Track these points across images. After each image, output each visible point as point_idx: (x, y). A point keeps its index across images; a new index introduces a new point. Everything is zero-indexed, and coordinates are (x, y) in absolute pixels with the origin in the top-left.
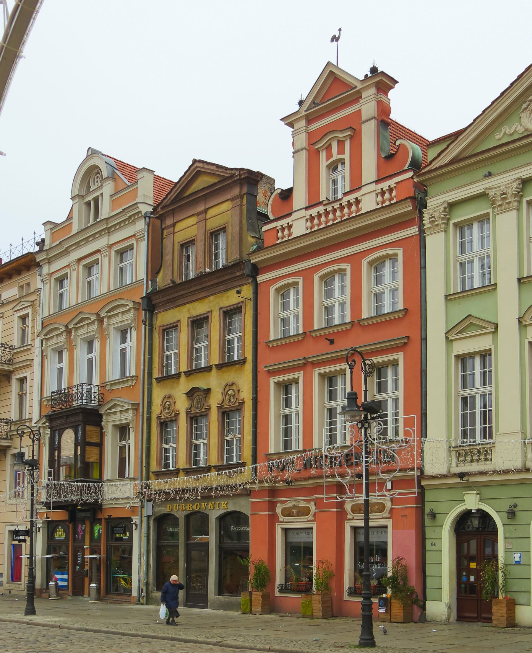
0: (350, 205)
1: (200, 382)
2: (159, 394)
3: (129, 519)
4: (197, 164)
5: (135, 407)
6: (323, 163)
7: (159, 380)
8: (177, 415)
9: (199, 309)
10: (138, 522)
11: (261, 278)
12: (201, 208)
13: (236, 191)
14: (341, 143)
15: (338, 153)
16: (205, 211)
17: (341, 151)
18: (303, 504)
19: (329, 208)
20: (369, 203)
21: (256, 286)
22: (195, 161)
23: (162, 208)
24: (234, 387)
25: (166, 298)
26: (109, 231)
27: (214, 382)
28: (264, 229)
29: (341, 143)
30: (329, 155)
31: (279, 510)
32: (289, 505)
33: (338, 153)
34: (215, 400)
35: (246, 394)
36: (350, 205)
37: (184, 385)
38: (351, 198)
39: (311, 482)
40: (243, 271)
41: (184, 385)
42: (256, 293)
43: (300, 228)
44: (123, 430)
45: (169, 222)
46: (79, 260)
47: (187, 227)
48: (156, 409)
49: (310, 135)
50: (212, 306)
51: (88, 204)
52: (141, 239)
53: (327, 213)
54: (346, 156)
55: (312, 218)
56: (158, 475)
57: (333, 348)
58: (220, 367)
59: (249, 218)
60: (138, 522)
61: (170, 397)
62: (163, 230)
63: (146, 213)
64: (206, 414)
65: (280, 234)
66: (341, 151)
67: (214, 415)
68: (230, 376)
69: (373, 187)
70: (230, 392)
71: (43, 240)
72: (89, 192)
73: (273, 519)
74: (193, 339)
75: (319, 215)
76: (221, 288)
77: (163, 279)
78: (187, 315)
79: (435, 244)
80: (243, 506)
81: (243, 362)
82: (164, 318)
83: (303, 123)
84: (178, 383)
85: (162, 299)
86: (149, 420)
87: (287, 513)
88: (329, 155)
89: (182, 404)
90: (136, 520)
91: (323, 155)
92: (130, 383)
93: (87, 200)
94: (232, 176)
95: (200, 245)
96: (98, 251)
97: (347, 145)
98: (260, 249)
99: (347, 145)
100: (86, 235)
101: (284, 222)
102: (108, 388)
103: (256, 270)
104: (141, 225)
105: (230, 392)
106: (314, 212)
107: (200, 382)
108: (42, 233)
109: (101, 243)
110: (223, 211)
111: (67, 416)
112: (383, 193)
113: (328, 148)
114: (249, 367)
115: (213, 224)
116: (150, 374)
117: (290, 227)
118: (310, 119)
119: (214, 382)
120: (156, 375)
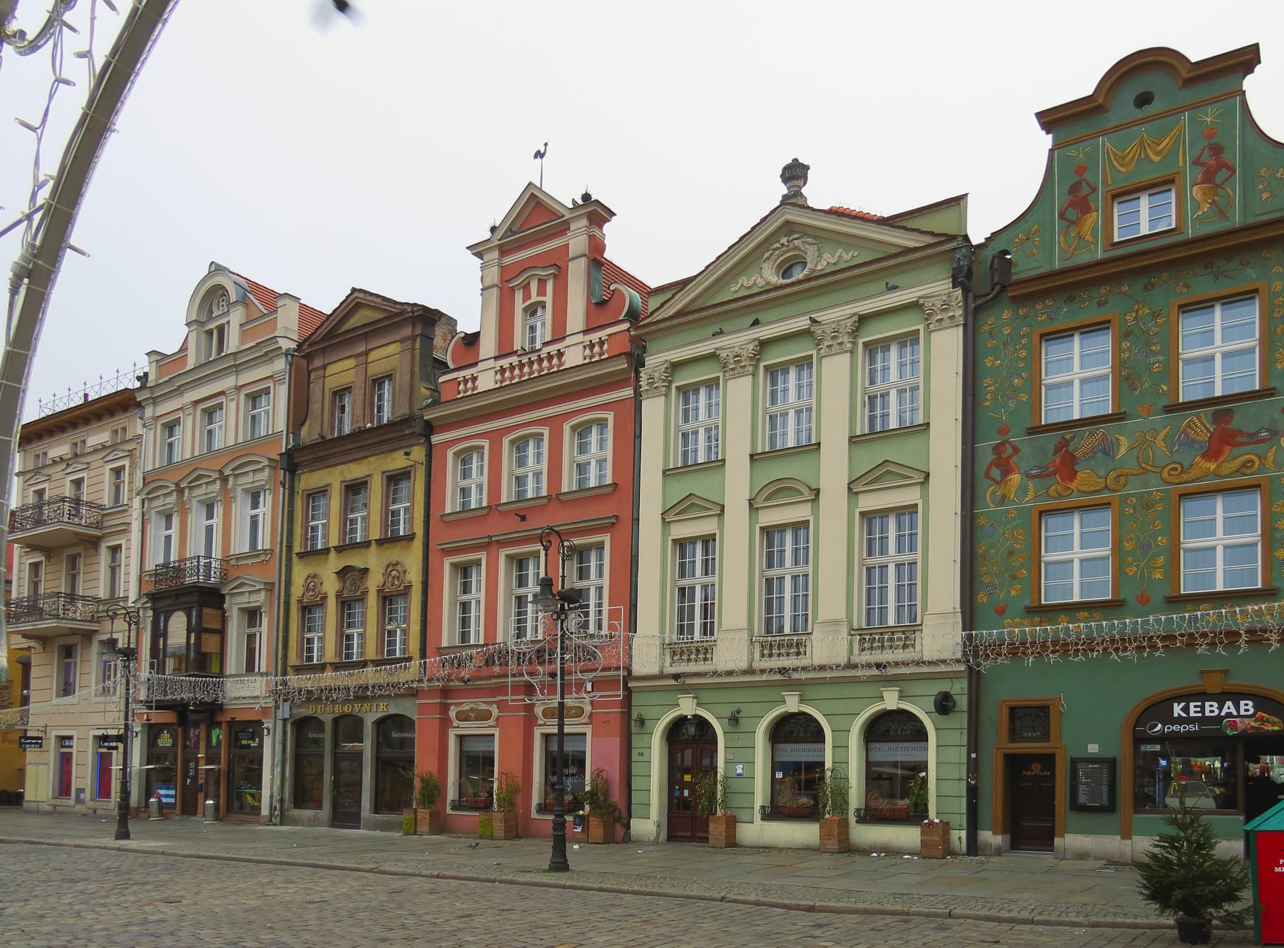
0: (550, 357)
1: (356, 560)
2: (300, 573)
3: (259, 723)
4: (356, 294)
5: (269, 588)
6: (519, 305)
7: (301, 556)
8: (324, 598)
9: (355, 471)
10: (271, 726)
11: (435, 439)
12: (361, 348)
13: (407, 331)
14: (542, 282)
15: (538, 295)
16: (367, 353)
17: (542, 292)
18: (483, 707)
19: (525, 360)
20: (574, 357)
21: (430, 448)
22: (354, 290)
23: (309, 346)
24: (399, 568)
25: (312, 456)
26: (237, 369)
27: (374, 561)
28: (441, 380)
29: (542, 282)
30: (527, 296)
31: (453, 713)
32: (467, 708)
33: (538, 295)
34: (373, 583)
35: (414, 575)
36: (550, 357)
37: (334, 563)
38: (553, 349)
39: (493, 681)
40: (414, 429)
41: (334, 563)
42: (429, 456)
43: (487, 381)
44: (252, 615)
45: (318, 363)
46: (196, 403)
47: (341, 370)
48: (297, 590)
49: (503, 269)
50: (373, 468)
51: (210, 333)
52: (281, 381)
53: (521, 366)
54: (548, 299)
55: (503, 370)
56: (298, 670)
57: (524, 526)
58: (380, 542)
59: (422, 365)
60: (271, 726)
61: (315, 576)
62: (310, 372)
63: (288, 350)
64: (362, 599)
65: (462, 387)
66: (542, 292)
67: (372, 600)
68: (394, 554)
69: (580, 338)
70: (394, 573)
71: (146, 374)
72: (210, 318)
73: (445, 723)
74: (347, 508)
75: (512, 368)
76: (385, 447)
77: (309, 432)
78: (340, 478)
79: (653, 411)
80: (408, 708)
81: (410, 538)
82: (310, 480)
83: (495, 254)
84: (327, 560)
85: (307, 458)
86: (287, 604)
87: (463, 717)
88: (527, 296)
89: (331, 586)
90: (268, 724)
91: (519, 296)
92: (263, 557)
93: (208, 328)
94: (403, 312)
95: (358, 394)
96: (222, 393)
97: (550, 286)
98: (436, 403)
99: (550, 286)
100: (206, 372)
101: (467, 373)
102: (233, 562)
103: (430, 428)
104: (280, 365)
105: (394, 573)
106: (505, 363)
107: (356, 560)
108: (144, 365)
109: (227, 383)
110: (388, 355)
111: (177, 596)
112: (592, 346)
113: (526, 287)
114: (418, 543)
115: (375, 369)
116: (290, 548)
117: (474, 379)
118: (504, 250)
119: (374, 561)
120: (297, 548)
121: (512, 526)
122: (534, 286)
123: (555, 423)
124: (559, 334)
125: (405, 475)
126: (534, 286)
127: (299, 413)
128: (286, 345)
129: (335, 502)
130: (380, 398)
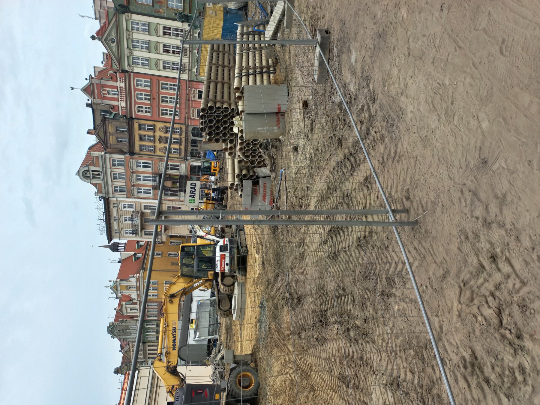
1: (157, 138)
2: (158, 153)
6: (108, 96)
7: (154, 153)
9: (137, 138)
11: (134, 117)
12: (108, 134)
14: (103, 90)
17: (105, 90)
20: (122, 85)
27: (158, 134)
30: (106, 94)
34: (163, 135)
37: (157, 144)
38: (119, 89)
41: (157, 144)
43: (123, 104)
46: (112, 181)
50: (137, 133)
54: (107, 89)
55: (121, 101)
56: (180, 155)
66: (105, 90)
74: (145, 140)
79: (136, 70)
80: (190, 129)
81: (154, 125)
88: (106, 94)
89: (162, 145)
91: (105, 96)
95: (120, 135)
96: (111, 173)
97: (105, 89)
99: (105, 89)
100: (105, 179)
101: (120, 108)
103: (132, 118)
104: (108, 156)
106: (120, 99)
107: (157, 138)
113: (104, 94)
114: (156, 123)
116: (152, 155)
119: (158, 134)
120: (153, 154)
121: (155, 101)
122: (104, 92)
123: (135, 90)
124: (116, 87)
125: (140, 125)
126: (104, 92)
127: (121, 152)
128: (103, 153)
129: (144, 143)
130: (120, 131)
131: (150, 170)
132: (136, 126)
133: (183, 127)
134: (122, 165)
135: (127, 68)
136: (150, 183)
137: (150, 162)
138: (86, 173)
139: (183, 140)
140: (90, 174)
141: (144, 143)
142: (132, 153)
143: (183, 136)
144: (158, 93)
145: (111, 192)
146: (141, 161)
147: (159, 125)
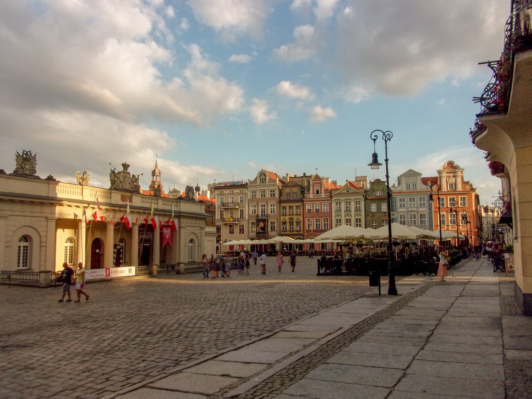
2: (282, 218)
9: (291, 205)
34: (295, 220)
47: (287, 190)
48: (282, 220)
50: (294, 205)
56: (282, 231)
64: (293, 222)
68: (298, 216)
79: (333, 204)
89: (288, 220)
110: (295, 189)
114: (302, 216)
119: (295, 217)
125: (299, 206)
127: (281, 195)
129: (288, 209)
131: (269, 212)
132: (299, 204)
133: (302, 232)
134: (271, 196)
135: (333, 199)
136: (260, 213)
137: (275, 213)
138: (263, 174)
139: (293, 233)
140: (263, 177)
141: (288, 209)
142: (280, 202)
143: (295, 233)
144: (321, 217)
145: (252, 189)
146: (275, 207)
147: (301, 219)
